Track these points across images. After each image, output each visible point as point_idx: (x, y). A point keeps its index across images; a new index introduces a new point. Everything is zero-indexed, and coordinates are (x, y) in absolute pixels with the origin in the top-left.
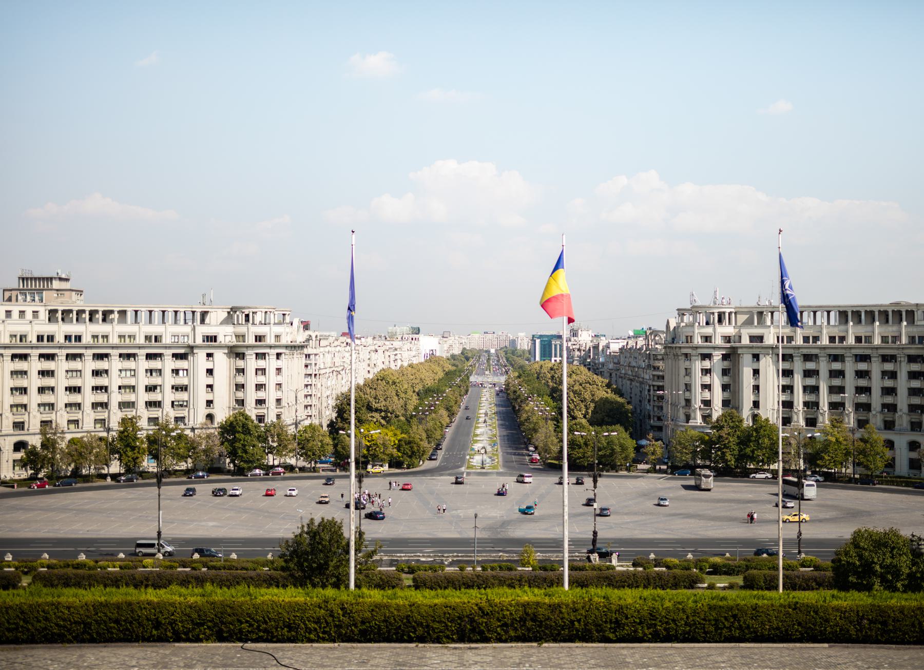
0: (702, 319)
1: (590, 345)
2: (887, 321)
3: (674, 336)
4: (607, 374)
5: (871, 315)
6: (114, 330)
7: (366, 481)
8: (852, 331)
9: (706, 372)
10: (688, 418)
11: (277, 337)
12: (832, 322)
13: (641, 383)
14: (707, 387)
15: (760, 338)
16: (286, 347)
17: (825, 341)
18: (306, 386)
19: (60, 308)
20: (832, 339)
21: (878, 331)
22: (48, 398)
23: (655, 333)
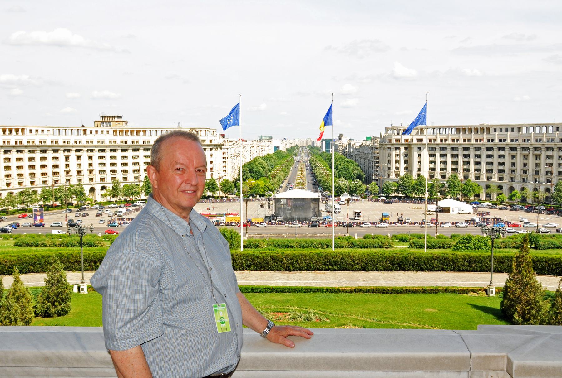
0: (396, 132)
1: (347, 143)
2: (478, 133)
3: (383, 140)
4: (354, 157)
5: (470, 130)
6: (141, 138)
7: (249, 203)
8: (462, 137)
9: (397, 155)
10: (389, 175)
11: (211, 141)
12: (453, 133)
13: (369, 160)
14: (397, 162)
15: (421, 140)
16: (215, 145)
17: (450, 141)
18: (224, 162)
19: (118, 129)
20: (453, 140)
21: (473, 137)
22: (114, 168)
23: (375, 138)
